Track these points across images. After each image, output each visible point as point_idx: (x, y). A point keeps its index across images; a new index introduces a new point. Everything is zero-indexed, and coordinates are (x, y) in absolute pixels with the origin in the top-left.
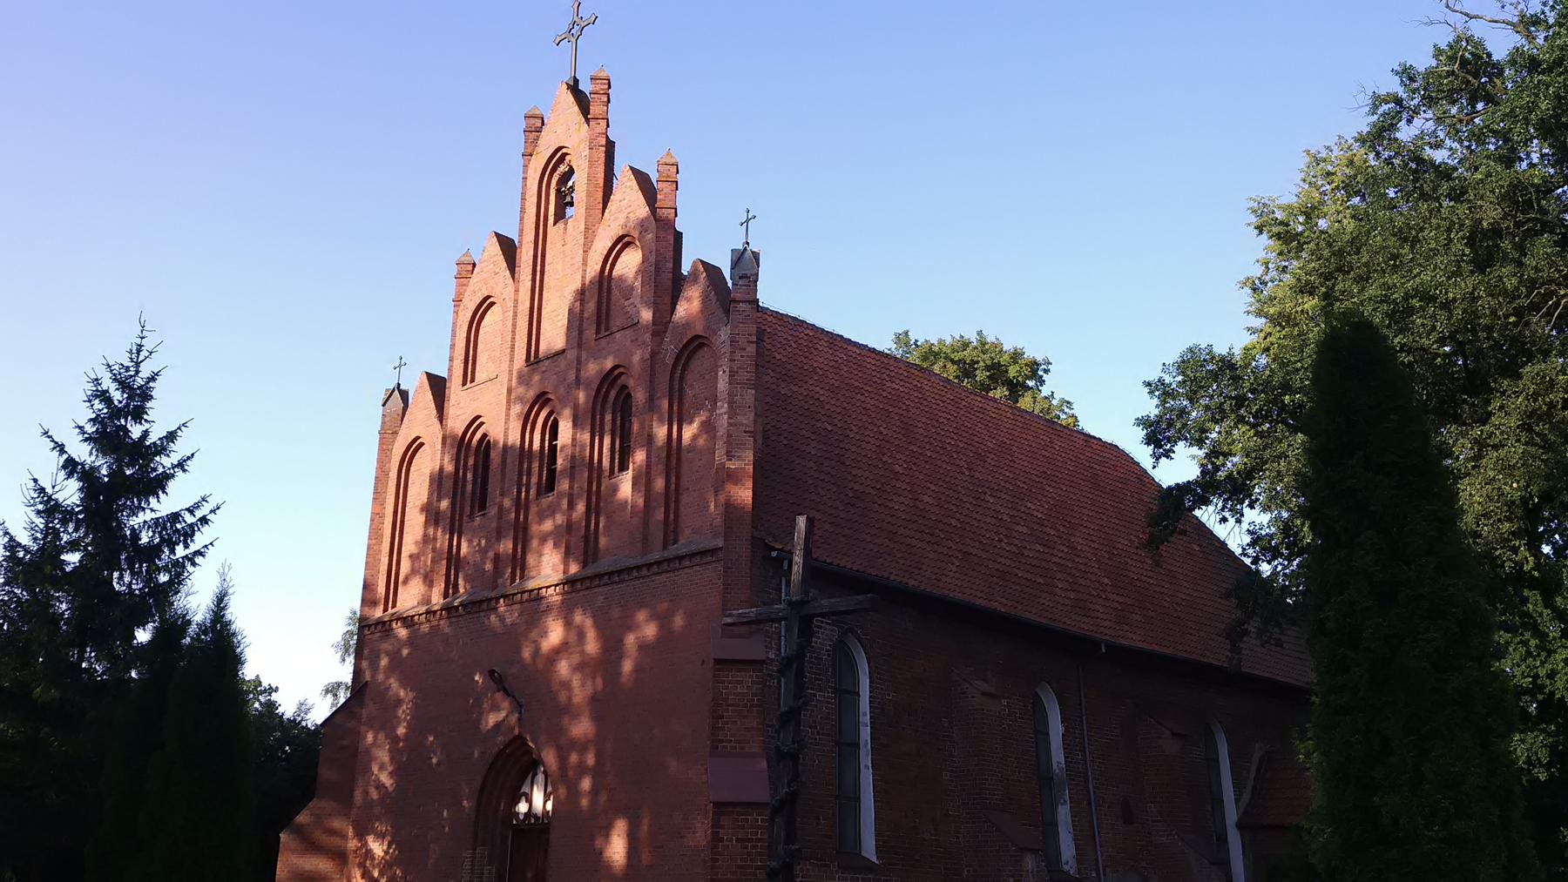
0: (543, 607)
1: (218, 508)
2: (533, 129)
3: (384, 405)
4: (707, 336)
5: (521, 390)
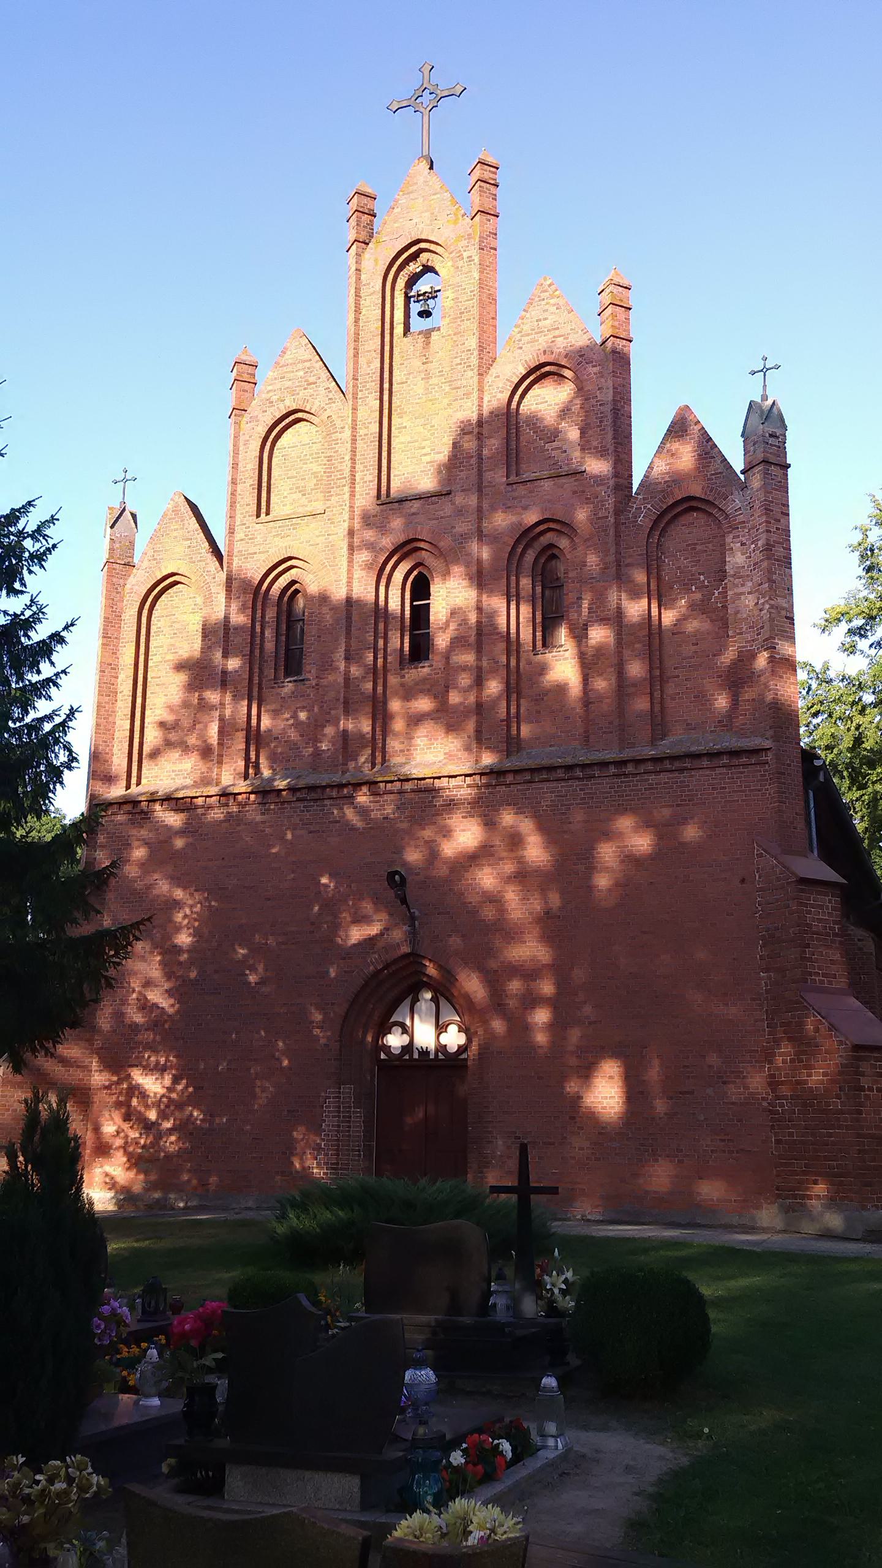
0: (439, 802)
1: (72, 625)
2: (367, 211)
3: (112, 527)
4: (711, 498)
5: (369, 535)
